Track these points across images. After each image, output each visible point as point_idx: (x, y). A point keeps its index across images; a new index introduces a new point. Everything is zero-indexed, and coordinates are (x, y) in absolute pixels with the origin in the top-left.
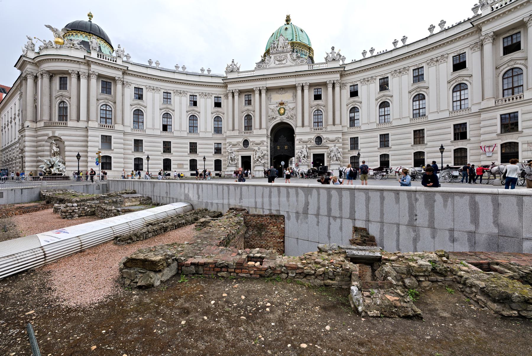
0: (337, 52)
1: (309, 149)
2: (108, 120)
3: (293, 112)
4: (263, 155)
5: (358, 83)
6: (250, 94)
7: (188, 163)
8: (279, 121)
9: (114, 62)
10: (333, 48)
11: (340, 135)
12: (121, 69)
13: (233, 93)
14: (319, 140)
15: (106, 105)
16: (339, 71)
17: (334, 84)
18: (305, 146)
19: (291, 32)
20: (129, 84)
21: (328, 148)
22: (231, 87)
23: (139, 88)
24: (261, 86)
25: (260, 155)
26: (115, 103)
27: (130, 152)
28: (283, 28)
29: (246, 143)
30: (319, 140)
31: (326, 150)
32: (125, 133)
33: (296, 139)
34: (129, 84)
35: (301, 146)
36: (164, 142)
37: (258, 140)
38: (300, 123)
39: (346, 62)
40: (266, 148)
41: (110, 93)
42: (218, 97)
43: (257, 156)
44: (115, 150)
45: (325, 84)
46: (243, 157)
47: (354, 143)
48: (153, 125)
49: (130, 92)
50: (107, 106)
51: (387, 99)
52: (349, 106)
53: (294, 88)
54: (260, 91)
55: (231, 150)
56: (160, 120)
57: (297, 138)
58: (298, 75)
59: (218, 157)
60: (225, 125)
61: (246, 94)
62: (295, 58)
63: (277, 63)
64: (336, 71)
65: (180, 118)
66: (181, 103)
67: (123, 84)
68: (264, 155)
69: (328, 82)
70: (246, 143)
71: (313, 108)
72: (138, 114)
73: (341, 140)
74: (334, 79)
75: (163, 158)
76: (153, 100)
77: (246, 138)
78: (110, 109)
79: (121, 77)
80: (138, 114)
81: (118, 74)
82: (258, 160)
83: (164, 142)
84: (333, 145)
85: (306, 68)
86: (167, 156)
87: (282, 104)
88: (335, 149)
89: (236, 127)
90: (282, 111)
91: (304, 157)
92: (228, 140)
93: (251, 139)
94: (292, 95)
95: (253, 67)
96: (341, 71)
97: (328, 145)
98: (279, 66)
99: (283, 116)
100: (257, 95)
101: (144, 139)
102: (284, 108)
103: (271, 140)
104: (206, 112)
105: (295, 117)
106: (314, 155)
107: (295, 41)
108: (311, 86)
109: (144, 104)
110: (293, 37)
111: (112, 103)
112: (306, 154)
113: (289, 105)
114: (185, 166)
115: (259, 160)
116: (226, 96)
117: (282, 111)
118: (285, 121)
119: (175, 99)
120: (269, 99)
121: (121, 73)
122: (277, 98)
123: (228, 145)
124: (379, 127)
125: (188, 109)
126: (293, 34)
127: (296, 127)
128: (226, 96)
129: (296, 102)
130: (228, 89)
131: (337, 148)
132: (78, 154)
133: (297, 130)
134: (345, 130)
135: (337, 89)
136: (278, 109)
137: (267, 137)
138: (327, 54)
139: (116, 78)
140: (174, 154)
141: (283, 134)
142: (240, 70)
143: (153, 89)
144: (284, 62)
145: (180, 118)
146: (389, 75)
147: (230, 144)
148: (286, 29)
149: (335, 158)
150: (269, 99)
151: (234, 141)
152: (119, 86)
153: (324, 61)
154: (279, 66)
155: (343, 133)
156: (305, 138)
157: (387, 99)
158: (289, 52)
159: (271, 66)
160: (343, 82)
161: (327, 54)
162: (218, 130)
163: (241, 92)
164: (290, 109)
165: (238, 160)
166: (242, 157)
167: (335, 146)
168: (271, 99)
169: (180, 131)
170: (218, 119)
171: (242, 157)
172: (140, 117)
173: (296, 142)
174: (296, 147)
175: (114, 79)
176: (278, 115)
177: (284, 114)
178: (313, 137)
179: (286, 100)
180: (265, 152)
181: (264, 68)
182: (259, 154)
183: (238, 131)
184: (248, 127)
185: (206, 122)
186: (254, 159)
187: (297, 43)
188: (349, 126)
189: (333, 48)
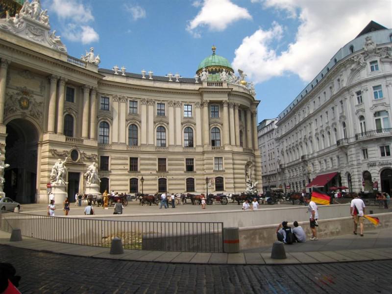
8: (20, 117)
14: (74, 154)
16: (98, 78)
30: (74, 154)
53: (48, 78)
91: (61, 176)
94: (40, 84)
97: (85, 163)
99: (25, 111)
102: (28, 100)
113: (35, 97)
118: (28, 118)
132: (142, 178)
136: (19, 98)
164: (36, 102)
176: (18, 107)
177: (27, 108)
179: (32, 89)
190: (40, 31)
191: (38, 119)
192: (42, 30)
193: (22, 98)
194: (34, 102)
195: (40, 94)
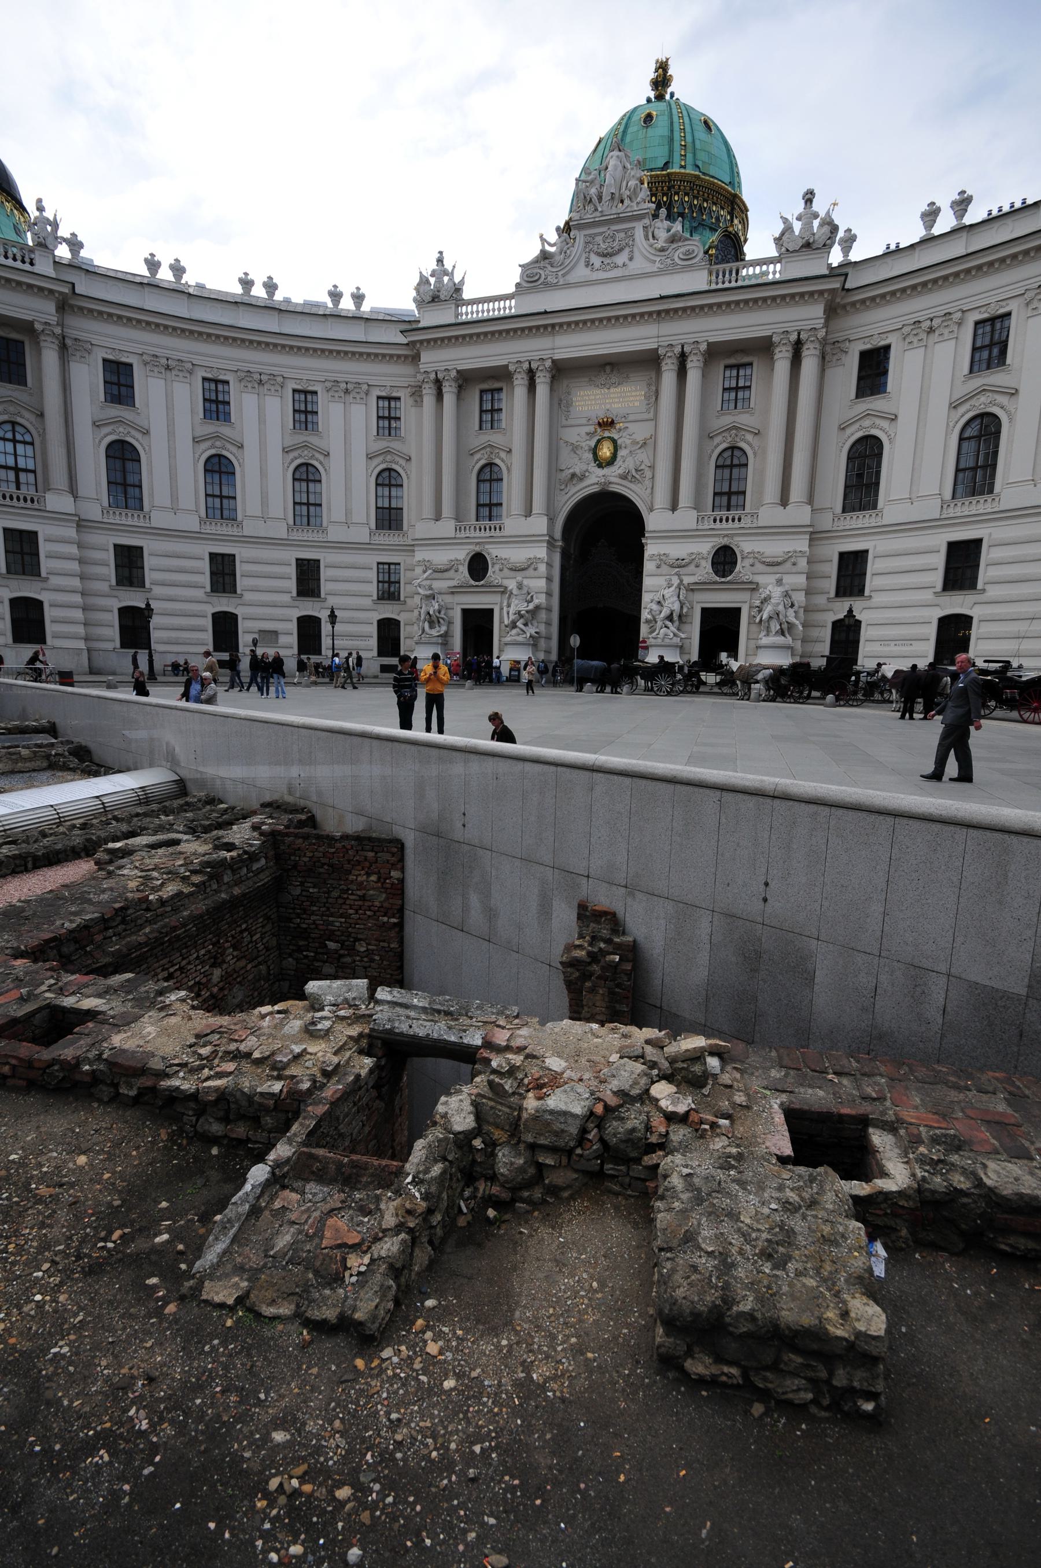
0: (822, 214)
1: (691, 589)
2: (23, 476)
3: (643, 456)
4: (531, 606)
5: (892, 339)
6: (497, 385)
7: (293, 626)
8: (595, 489)
9: (27, 267)
10: (809, 197)
11: (802, 544)
12: (51, 291)
13: (438, 383)
14: (724, 560)
15: (14, 424)
16: (821, 293)
17: (798, 346)
18: (676, 581)
19: (666, 132)
20: (85, 348)
21: (754, 587)
22: (432, 360)
23: (118, 364)
24: (536, 356)
25: (523, 607)
26: (41, 415)
27: (103, 587)
28: (635, 118)
29: (478, 566)
30: (724, 560)
31: (745, 596)
32: (82, 524)
33: (647, 554)
34: (85, 348)
35: (661, 581)
36: (213, 556)
37: (518, 555)
38: (662, 497)
39: (857, 255)
40: (542, 583)
41: (22, 381)
42: (389, 399)
43: (512, 610)
44: (55, 581)
45: (764, 347)
46: (468, 614)
47: (852, 572)
48: (174, 497)
49: (88, 379)
50: (18, 428)
51: (993, 403)
52: (849, 431)
54: (531, 374)
55: (431, 588)
56: (196, 481)
57: (651, 549)
58: (667, 311)
59: (388, 611)
60: (414, 498)
61: (485, 386)
62: (660, 244)
63: (596, 261)
64: (811, 294)
65: (263, 473)
66: (262, 420)
67: (63, 347)
68: (538, 608)
69: (775, 339)
70: (478, 566)
71: (717, 440)
72: (122, 457)
73: (803, 563)
74: (800, 325)
75: (211, 610)
76: (170, 408)
77: (478, 549)
78: (28, 438)
79: (53, 319)
80: (122, 457)
81: (41, 311)
82: (514, 625)
83: (213, 556)
84: (772, 579)
85: (698, 280)
86: (224, 604)
87: (607, 424)
88: (777, 592)
89: (447, 509)
90: (606, 451)
91: (670, 618)
92: (420, 555)
93: (493, 552)
95: (508, 281)
96: (833, 291)
98: (602, 275)
99: (606, 471)
100: (520, 391)
101: (149, 546)
103: (565, 555)
104: (347, 455)
105: (648, 474)
106: (704, 610)
107: (676, 169)
108: (714, 352)
109: (141, 421)
110: (671, 151)
111: (32, 418)
112: (676, 607)
114: (283, 640)
115: (519, 624)
116: (417, 393)
117: (606, 451)
119: (244, 404)
120: (559, 404)
121: (50, 307)
122: (591, 401)
123: (419, 570)
124: (951, 512)
125: (289, 442)
126: (671, 140)
127: (651, 510)
128: (417, 393)
129: (655, 418)
130: (423, 367)
131: (787, 587)
133: (653, 521)
134: (826, 522)
135: (809, 365)
136: (593, 443)
137: (551, 544)
138: (785, 220)
139: (38, 327)
140: (248, 596)
141: (603, 539)
142: (467, 295)
143: (168, 368)
144: (620, 259)
145: (263, 473)
146: (1013, 306)
147: (427, 565)
148: (649, 117)
149: (775, 626)
150: (559, 404)
151: (441, 557)
152: (50, 357)
153: (772, 252)
154: (602, 275)
155: (815, 536)
156: (678, 550)
157: (993, 403)
158: (639, 218)
159: (572, 278)
160: (833, 337)
161: (785, 220)
162: (389, 518)
163: (465, 379)
164: (635, 443)
165: (450, 623)
166: (466, 613)
167: (779, 582)
168: (569, 405)
169: (264, 519)
170: (388, 479)
171: (466, 613)
172: (129, 465)
173: (648, 566)
174: (647, 582)
175: (27, 327)
176: (593, 467)
177: (611, 461)
178: (706, 548)
180: (540, 599)
181: (548, 286)
182: (518, 605)
183: (452, 524)
184: (489, 508)
185: (348, 489)
186: (501, 621)
187: (683, 178)
188: (839, 508)
189: (809, 197)
190: (622, 235)
191: (639, 482)
192: (626, 231)
193: (599, 441)
194: (628, 442)
195: (646, 416)
